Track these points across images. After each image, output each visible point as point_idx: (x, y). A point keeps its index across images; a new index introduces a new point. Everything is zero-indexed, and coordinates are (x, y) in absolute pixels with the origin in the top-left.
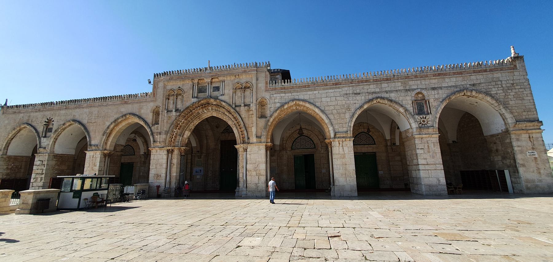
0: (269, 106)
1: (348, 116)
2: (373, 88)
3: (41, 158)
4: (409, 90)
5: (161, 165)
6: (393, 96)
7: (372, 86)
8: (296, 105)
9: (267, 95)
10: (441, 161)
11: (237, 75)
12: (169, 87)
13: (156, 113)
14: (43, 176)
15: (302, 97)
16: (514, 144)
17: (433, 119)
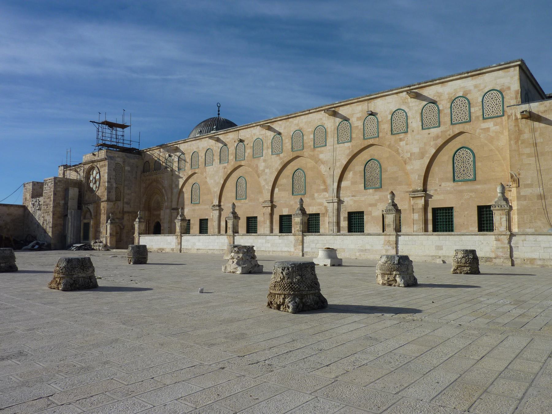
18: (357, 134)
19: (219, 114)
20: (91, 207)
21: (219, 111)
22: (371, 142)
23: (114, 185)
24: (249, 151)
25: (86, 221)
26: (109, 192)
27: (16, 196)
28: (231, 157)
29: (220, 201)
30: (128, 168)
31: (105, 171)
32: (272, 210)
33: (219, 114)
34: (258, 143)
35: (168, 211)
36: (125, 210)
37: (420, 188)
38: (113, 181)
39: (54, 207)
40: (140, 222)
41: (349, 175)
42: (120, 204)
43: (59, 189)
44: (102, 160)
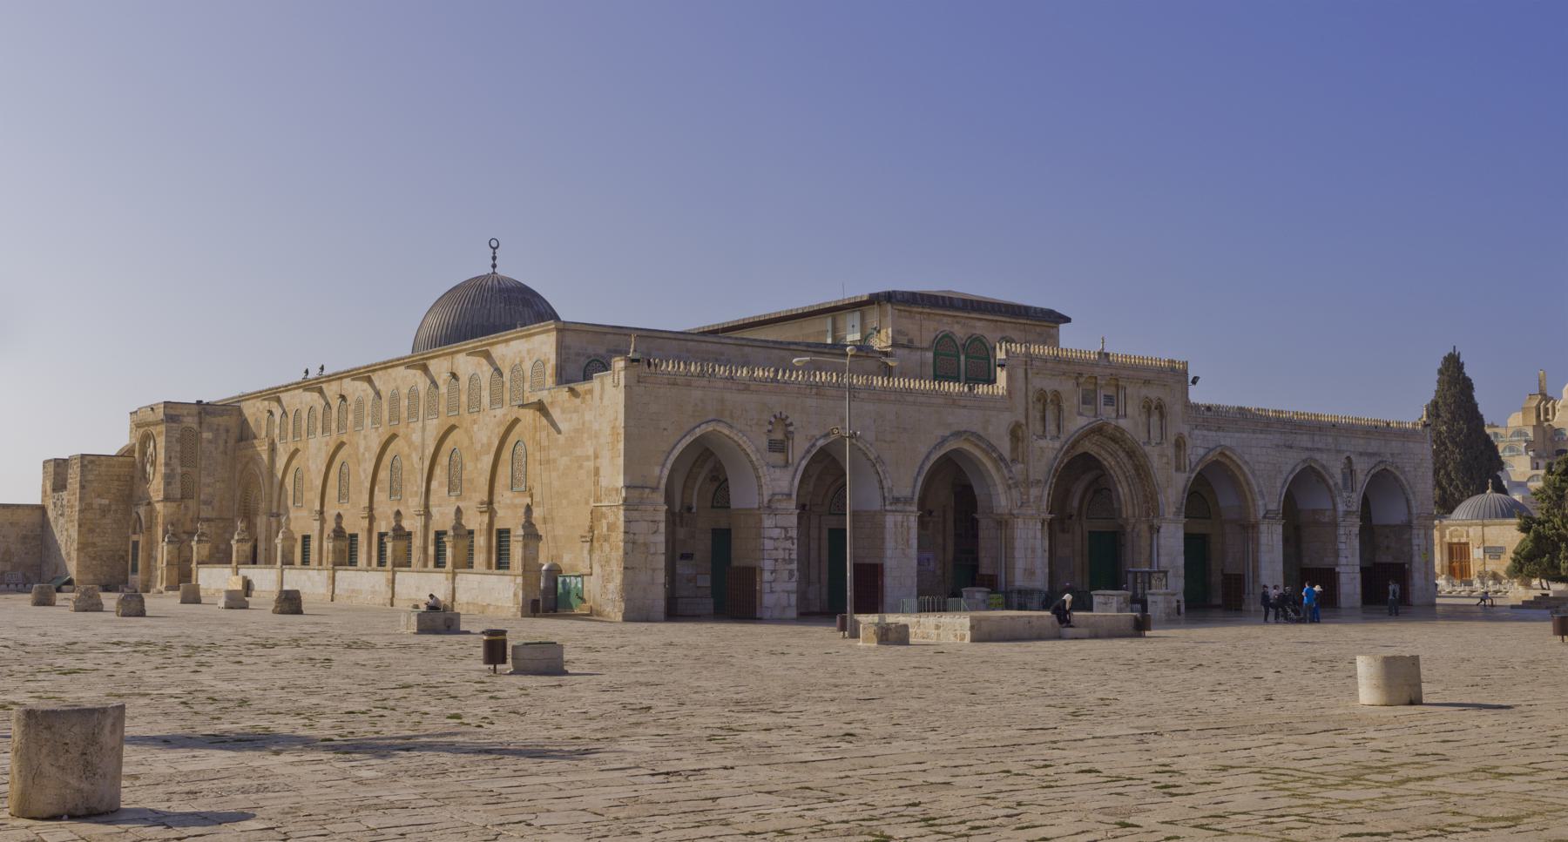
0: (1189, 452)
1: (1279, 484)
2: (1305, 441)
3: (782, 520)
4: (1338, 451)
5: (1033, 550)
6: (1323, 458)
7: (1305, 438)
8: (1222, 454)
9: (1185, 430)
10: (1357, 561)
11: (1147, 382)
12: (1038, 383)
13: (1016, 434)
14: (794, 566)
15: (1227, 442)
16: (1415, 542)
17: (1356, 499)
18: (442, 408)
19: (494, 266)
20: (142, 511)
21: (494, 258)
22: (453, 421)
23: (179, 470)
24: (351, 417)
25: (135, 538)
26: (168, 484)
27: (28, 490)
28: (334, 426)
29: (322, 505)
30: (207, 435)
31: (161, 442)
32: (371, 524)
33: (494, 266)
34: (360, 403)
35: (264, 518)
36: (203, 515)
37: (486, 499)
38: (175, 462)
39: (81, 511)
40: (199, 541)
41: (438, 471)
42: (192, 504)
43: (90, 477)
44: (156, 424)
